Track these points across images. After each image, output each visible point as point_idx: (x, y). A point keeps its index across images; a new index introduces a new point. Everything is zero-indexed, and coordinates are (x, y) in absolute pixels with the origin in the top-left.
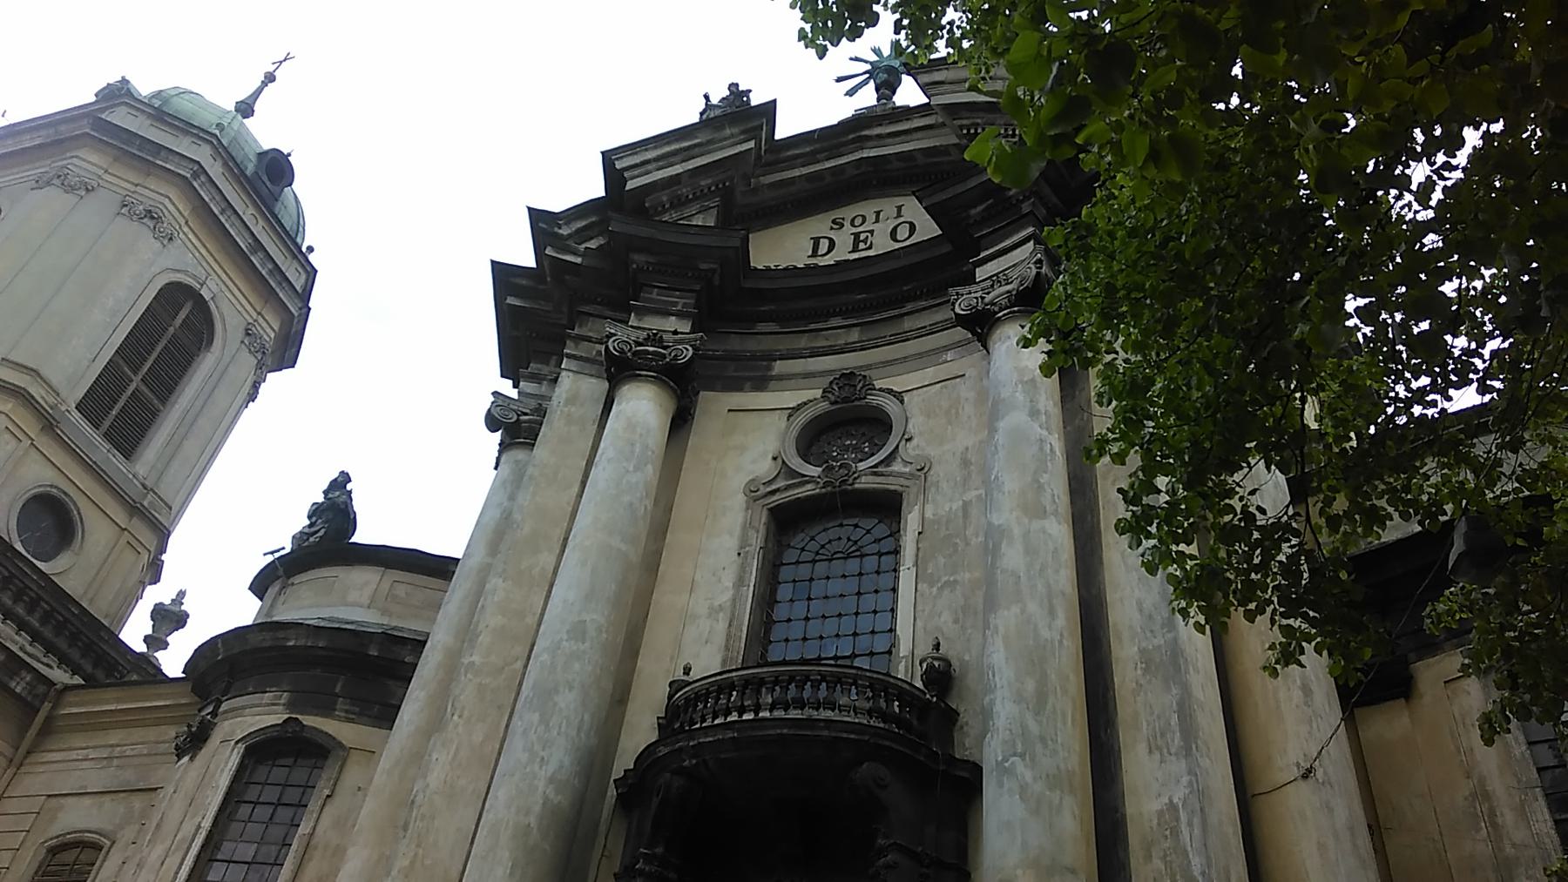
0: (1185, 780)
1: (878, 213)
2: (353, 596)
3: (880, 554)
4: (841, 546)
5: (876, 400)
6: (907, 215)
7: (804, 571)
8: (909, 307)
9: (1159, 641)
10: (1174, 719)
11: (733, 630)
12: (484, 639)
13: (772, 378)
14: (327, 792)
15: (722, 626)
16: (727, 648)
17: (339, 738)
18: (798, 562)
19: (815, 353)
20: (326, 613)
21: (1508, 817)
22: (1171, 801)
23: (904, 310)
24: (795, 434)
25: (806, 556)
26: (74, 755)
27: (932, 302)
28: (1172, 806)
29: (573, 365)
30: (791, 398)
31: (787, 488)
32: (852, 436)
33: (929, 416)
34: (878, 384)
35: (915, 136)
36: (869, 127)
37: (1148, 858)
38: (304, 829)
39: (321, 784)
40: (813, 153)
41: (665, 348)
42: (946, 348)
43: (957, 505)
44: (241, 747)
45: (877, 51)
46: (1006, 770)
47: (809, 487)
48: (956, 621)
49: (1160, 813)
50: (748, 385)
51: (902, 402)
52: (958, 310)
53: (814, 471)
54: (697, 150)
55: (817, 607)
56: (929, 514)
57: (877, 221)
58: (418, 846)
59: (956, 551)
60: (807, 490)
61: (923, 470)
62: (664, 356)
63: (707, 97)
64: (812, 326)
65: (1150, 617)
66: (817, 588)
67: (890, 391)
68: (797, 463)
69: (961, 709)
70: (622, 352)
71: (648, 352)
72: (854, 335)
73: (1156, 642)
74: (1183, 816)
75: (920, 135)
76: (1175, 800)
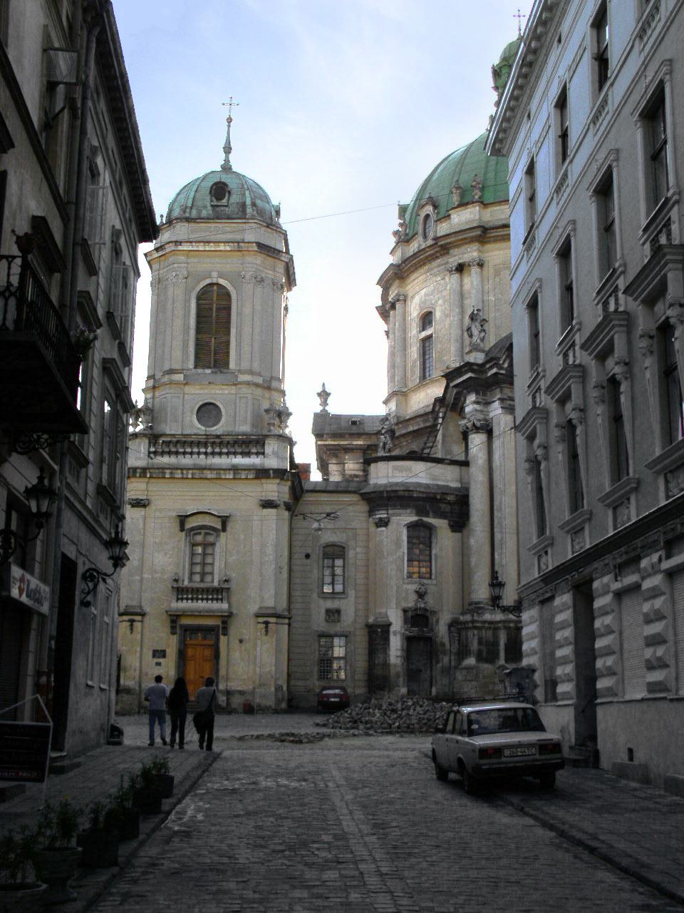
20: (414, 480)
38: (434, 552)
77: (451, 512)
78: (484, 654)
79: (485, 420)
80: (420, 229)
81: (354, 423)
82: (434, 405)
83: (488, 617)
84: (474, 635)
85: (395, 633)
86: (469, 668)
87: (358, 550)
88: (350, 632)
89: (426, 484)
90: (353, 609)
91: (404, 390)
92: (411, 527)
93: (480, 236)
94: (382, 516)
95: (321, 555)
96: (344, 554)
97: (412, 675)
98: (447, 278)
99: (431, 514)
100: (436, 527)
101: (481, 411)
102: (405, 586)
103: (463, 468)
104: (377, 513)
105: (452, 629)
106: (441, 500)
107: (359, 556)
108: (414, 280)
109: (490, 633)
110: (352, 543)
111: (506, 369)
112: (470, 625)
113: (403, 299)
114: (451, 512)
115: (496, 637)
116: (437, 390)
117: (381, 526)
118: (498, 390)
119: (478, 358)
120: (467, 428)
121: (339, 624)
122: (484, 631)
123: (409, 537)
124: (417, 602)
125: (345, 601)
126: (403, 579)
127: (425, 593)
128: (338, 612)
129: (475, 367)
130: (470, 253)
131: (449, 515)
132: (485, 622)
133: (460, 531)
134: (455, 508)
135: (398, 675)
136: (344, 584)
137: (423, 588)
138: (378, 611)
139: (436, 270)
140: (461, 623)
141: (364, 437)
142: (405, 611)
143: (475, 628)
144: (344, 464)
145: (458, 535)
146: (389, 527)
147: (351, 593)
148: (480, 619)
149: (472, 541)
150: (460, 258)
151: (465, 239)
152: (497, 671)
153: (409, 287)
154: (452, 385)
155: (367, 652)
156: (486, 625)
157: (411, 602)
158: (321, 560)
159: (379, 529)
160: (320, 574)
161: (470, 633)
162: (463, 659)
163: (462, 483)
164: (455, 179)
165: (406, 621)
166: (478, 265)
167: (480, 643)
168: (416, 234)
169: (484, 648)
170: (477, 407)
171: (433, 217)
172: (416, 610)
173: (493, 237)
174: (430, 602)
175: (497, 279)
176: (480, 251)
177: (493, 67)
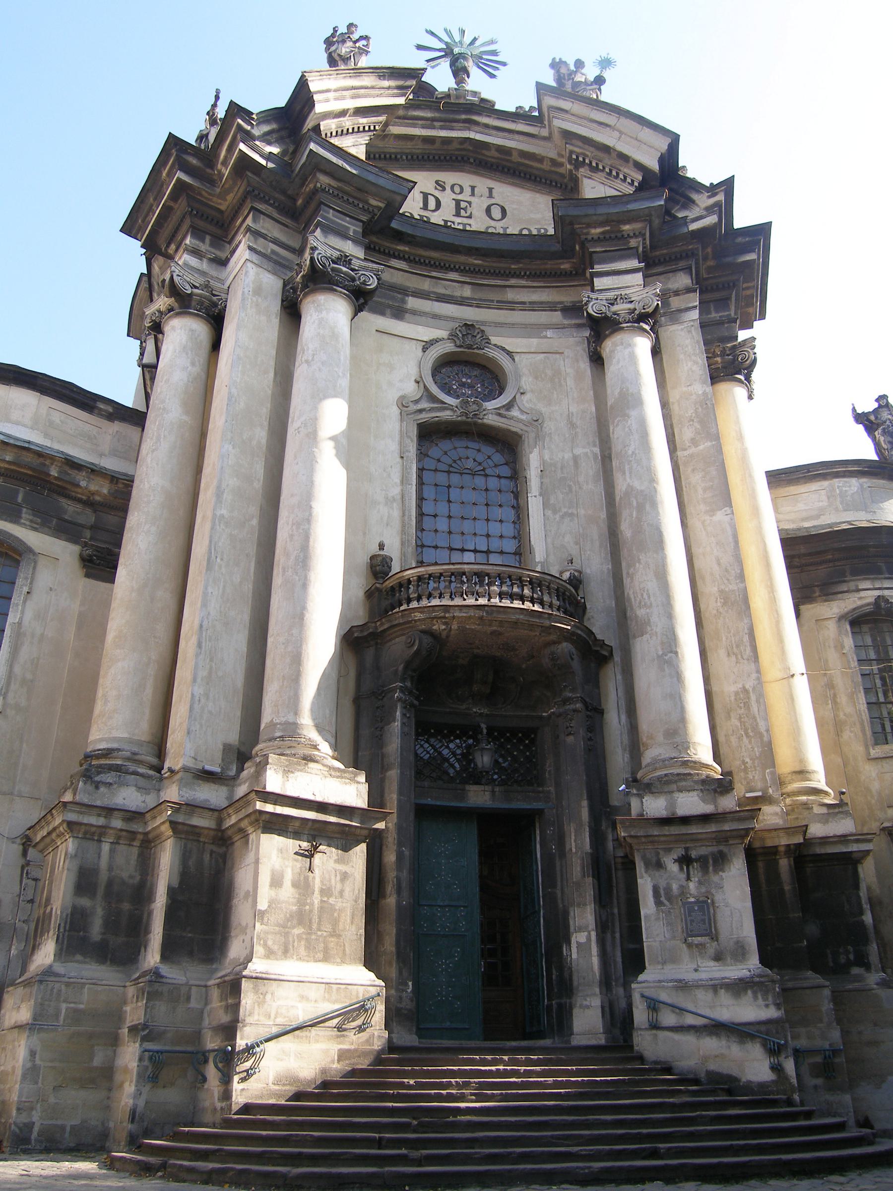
0: (754, 675)
1: (473, 188)
2: (15, 415)
3: (499, 477)
4: (470, 464)
6: (497, 199)
7: (442, 478)
8: (513, 282)
9: (733, 587)
10: (746, 638)
11: (406, 518)
12: (227, 497)
13: (406, 311)
14: (26, 589)
15: (396, 513)
16: (403, 532)
17: (29, 544)
18: (436, 470)
19: (442, 298)
21: (843, 699)
22: (744, 687)
23: (507, 283)
25: (441, 467)
27: (530, 284)
28: (745, 691)
29: (255, 258)
30: (427, 333)
31: (431, 410)
33: (536, 378)
34: (494, 340)
35: (516, 137)
36: (479, 114)
37: (728, 717)
38: (12, 618)
39: (19, 582)
40: (433, 120)
41: (353, 270)
43: (568, 456)
45: (448, 33)
46: (666, 662)
47: (448, 413)
48: (577, 543)
49: (737, 693)
50: (388, 311)
51: (514, 360)
52: (590, 311)
54: (362, 91)
55: (456, 509)
56: (547, 457)
57: (473, 194)
58: (211, 660)
59: (571, 490)
60: (446, 415)
61: (537, 422)
62: (353, 280)
63: (335, 30)
64: (434, 274)
65: (727, 570)
66: (454, 494)
67: (503, 349)
68: (435, 390)
69: (588, 606)
70: (324, 266)
71: (340, 271)
72: (467, 292)
73: (731, 587)
74: (753, 698)
75: (521, 138)
76: (747, 687)
77: (92, 528)
78: (96, 930)
79: (207, 286)
83: (129, 797)
99: (26, 514)
100: (30, 550)
101: (203, 273)
106: (63, 489)
109: (128, 856)
111: (269, 157)
122: (106, 847)
129: (194, 161)
131: (88, 534)
132: (109, 811)
148: (98, 803)
162: (35, 948)
167: (85, 881)
170: (193, 261)
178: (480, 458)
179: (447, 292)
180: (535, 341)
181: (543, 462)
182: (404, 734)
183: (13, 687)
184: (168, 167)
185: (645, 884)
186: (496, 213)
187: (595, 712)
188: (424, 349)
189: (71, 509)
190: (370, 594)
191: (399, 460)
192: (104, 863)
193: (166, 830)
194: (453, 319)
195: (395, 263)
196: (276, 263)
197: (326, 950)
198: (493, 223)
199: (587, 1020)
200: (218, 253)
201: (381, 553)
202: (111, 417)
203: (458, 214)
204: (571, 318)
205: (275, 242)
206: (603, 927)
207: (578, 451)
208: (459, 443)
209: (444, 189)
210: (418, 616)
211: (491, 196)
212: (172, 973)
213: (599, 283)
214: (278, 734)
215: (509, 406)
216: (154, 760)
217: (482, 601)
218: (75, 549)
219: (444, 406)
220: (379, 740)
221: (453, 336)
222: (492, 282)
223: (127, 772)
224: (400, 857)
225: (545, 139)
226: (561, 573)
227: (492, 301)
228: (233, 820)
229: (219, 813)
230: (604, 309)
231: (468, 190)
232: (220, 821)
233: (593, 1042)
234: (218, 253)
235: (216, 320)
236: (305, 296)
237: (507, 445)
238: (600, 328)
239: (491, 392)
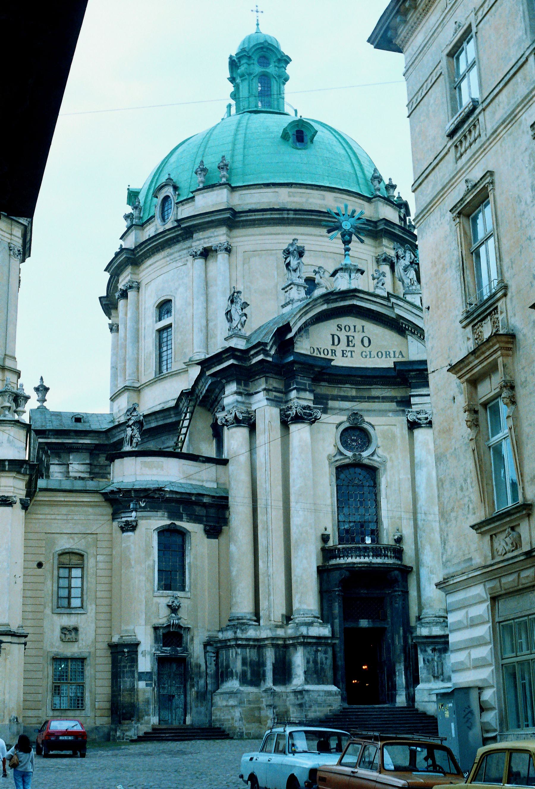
1: (355, 327)
5: (365, 426)
24: (339, 436)
26: (49, 517)
32: (354, 435)
34: (366, 419)
38: (187, 561)
39: (187, 545)
40: (337, 299)
41: (311, 410)
42: (390, 411)
44: (156, 532)
53: (349, 454)
57: (355, 331)
60: (347, 461)
62: (311, 415)
64: (340, 386)
67: (370, 424)
77: (207, 516)
79: (248, 412)
80: (157, 212)
81: (78, 420)
82: (179, 399)
83: (251, 633)
84: (236, 653)
85: (144, 654)
86: (232, 694)
87: (99, 558)
88: (90, 652)
89: (181, 484)
90: (93, 626)
91: (137, 385)
92: (162, 532)
93: (229, 218)
94: (129, 519)
95: (56, 562)
96: (83, 564)
97: (165, 701)
98: (189, 264)
101: (243, 403)
102: (155, 598)
103: (220, 467)
104: (123, 515)
105: (208, 648)
107: (101, 565)
108: (150, 265)
110: (92, 551)
112: (233, 643)
113: (136, 287)
114: (207, 516)
115: (261, 655)
116: (185, 383)
117: (127, 531)
118: (263, 379)
119: (240, 344)
120: (226, 421)
121: (76, 644)
122: (248, 650)
123: (159, 544)
124: (169, 618)
125: (83, 617)
126: (154, 591)
127: (179, 607)
128: (76, 629)
130: (218, 237)
131: (205, 519)
133: (217, 538)
134: (213, 512)
135: (147, 702)
136: (82, 597)
137: (176, 602)
138: (124, 628)
139: (176, 255)
140: (220, 641)
141: (92, 435)
142: (156, 629)
143: (239, 646)
144: (68, 465)
145: (214, 541)
146: (137, 531)
147: (91, 608)
148: (244, 636)
149: (233, 548)
150: (205, 243)
151: (212, 221)
152: (264, 695)
153: (144, 273)
154: (208, 373)
155: (109, 675)
156: (251, 643)
157: (162, 617)
158: (56, 567)
159: (125, 534)
160: (55, 585)
161: (232, 652)
162: (222, 682)
163: (217, 484)
164: (198, 161)
165: (156, 640)
166: (226, 249)
167: (244, 663)
168: (153, 217)
169: (248, 669)
170: (239, 398)
171: (174, 199)
172: (169, 626)
173: (242, 221)
174: (185, 618)
175: (246, 266)
176: (228, 236)
177: (231, 57)
178: (361, 477)
179: (345, 394)
180: (384, 419)
181: (387, 482)
182: (340, 607)
183: (192, 587)
184: (226, 355)
185: (421, 658)
186: (366, 343)
187: (406, 593)
188: (337, 428)
189: (198, 510)
190: (323, 549)
191: (329, 487)
192: (248, 655)
193: (270, 645)
194: (348, 409)
195: (323, 384)
196: (277, 401)
197: (323, 681)
198: (364, 349)
199: (401, 700)
200: (247, 389)
201: (327, 533)
202: (204, 462)
203: (348, 345)
204: (400, 406)
205: (276, 390)
206: (406, 669)
207: (402, 476)
208: (352, 470)
209: (341, 329)
210: (344, 566)
211: (363, 331)
212: (278, 689)
213: (413, 400)
214: (302, 613)
215: (373, 454)
216: (255, 618)
217: (367, 560)
218: (201, 526)
219: (346, 457)
220: (331, 608)
221: (348, 419)
222: (365, 387)
223: (250, 625)
224: (341, 650)
225: (389, 307)
226: (394, 536)
227: (364, 398)
228: (291, 642)
229: (284, 639)
230: (414, 418)
231: (352, 328)
232: (285, 641)
233: (403, 706)
234: (247, 389)
235: (252, 427)
236: (292, 423)
237: (372, 472)
238: (413, 426)
239: (365, 444)
